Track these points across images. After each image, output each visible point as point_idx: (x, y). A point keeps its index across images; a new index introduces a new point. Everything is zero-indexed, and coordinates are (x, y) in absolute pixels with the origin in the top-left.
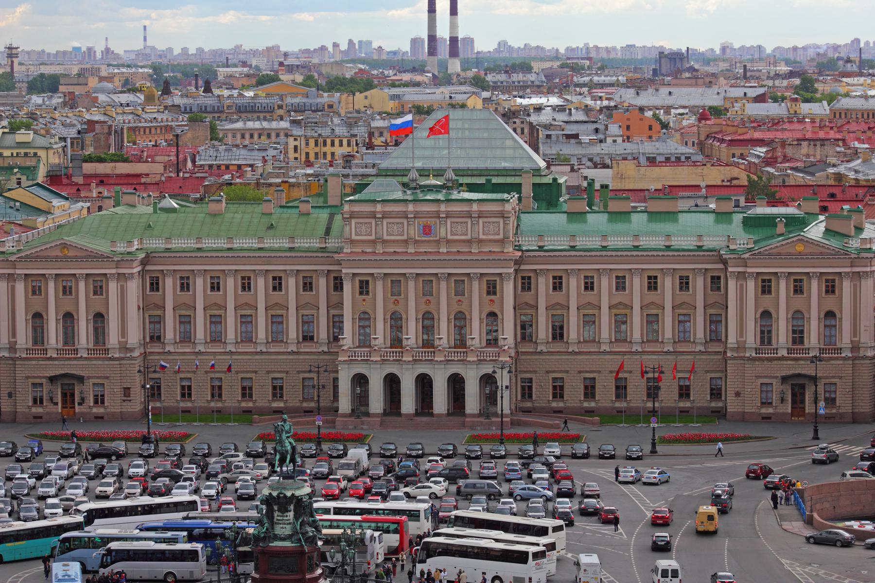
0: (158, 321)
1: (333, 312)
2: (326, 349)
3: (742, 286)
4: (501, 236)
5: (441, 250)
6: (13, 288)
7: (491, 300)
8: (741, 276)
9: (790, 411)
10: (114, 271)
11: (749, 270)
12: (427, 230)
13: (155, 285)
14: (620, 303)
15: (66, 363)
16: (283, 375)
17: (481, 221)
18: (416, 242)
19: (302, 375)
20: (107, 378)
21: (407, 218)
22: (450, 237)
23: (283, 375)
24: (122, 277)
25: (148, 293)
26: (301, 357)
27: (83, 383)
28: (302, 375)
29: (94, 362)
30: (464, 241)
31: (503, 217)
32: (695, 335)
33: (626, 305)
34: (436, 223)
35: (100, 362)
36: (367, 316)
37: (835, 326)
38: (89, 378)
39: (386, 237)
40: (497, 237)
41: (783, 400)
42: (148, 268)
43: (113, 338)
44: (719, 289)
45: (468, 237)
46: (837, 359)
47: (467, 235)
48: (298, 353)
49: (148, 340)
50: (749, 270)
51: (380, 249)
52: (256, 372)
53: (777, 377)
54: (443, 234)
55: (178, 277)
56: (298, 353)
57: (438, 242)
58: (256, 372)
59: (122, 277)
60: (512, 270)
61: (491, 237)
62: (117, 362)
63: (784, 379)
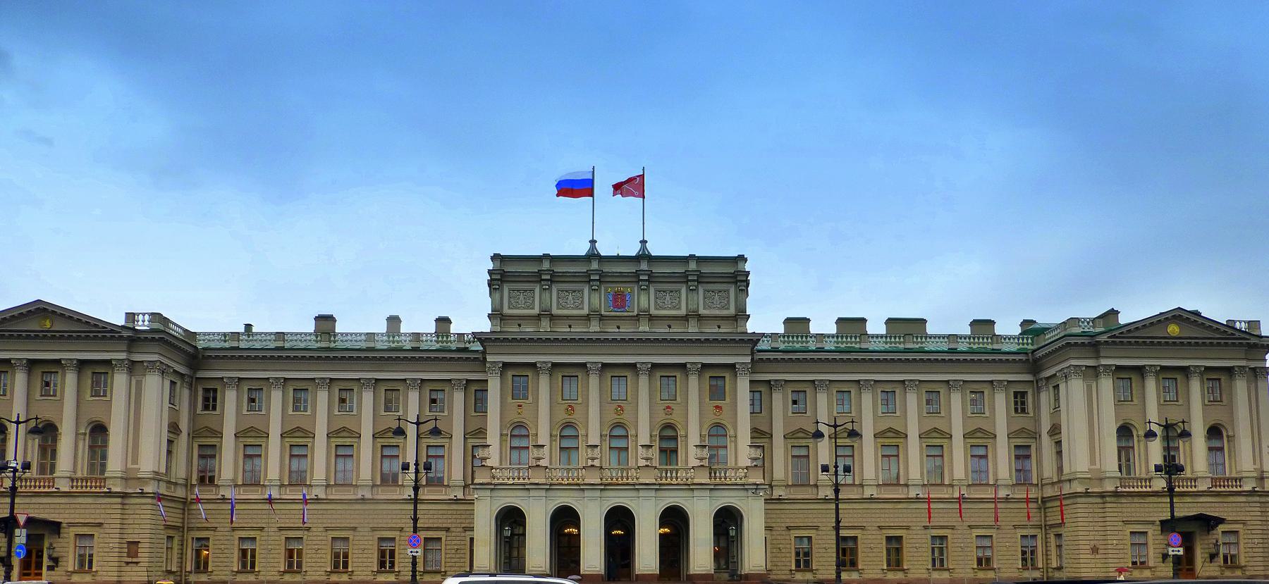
0: (209, 453)
1: (472, 442)
2: (460, 496)
4: (732, 311)
5: (641, 329)
7: (717, 407)
12: (619, 300)
13: (211, 400)
14: (890, 430)
15: (34, 500)
18: (602, 318)
20: (100, 525)
22: (653, 312)
25: (199, 411)
27: (59, 534)
29: (80, 500)
31: (736, 283)
32: (995, 474)
33: (897, 432)
34: (632, 291)
35: (90, 500)
36: (524, 432)
37: (1221, 449)
38: (71, 525)
39: (555, 311)
40: (725, 313)
42: (201, 374)
43: (114, 464)
44: (1023, 411)
45: (683, 312)
47: (679, 309)
51: (545, 325)
53: (1153, 523)
55: (246, 389)
57: (637, 318)
60: (748, 359)
61: (717, 312)
62: (119, 500)
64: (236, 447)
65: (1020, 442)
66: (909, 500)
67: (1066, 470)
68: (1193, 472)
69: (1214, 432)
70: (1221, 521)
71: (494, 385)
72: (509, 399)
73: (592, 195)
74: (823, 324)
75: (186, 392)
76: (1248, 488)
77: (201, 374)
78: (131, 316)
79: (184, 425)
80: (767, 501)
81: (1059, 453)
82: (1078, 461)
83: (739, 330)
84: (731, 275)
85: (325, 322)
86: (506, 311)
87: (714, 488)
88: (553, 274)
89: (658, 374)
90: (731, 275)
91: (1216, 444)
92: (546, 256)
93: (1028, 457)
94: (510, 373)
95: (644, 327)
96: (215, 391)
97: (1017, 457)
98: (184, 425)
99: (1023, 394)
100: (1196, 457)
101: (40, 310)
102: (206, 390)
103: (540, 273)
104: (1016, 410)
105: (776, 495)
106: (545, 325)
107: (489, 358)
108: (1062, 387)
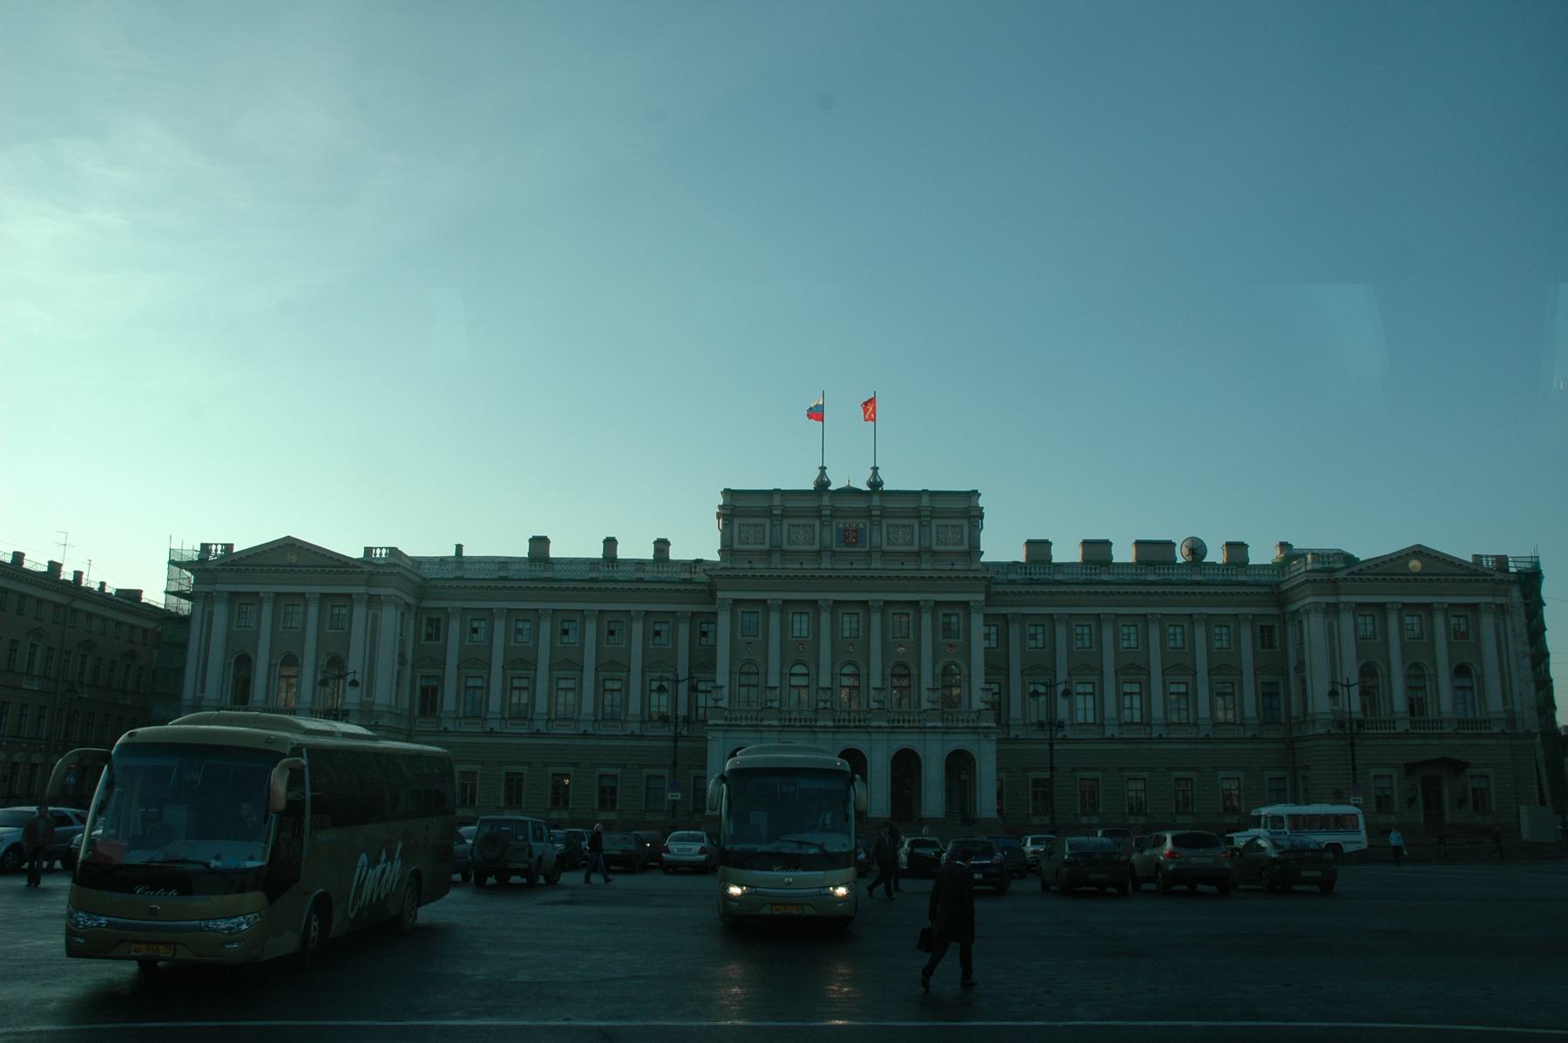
3: (1331, 625)
4: (965, 547)
5: (873, 565)
6: (211, 614)
8: (1333, 610)
9: (1421, 820)
10: (362, 590)
11: (1343, 599)
12: (850, 537)
13: (435, 629)
16: (617, 771)
17: (934, 523)
18: (834, 553)
19: (646, 772)
21: (820, 516)
22: (886, 547)
23: (617, 771)
24: (373, 601)
25: (423, 641)
26: (646, 743)
28: (646, 772)
30: (908, 553)
36: (753, 669)
37: (1471, 688)
39: (786, 547)
41: (1411, 802)
44: (1271, 646)
45: (915, 548)
46: (1481, 736)
48: (643, 737)
49: (416, 711)
50: (1343, 599)
51: (776, 561)
52: (575, 765)
54: (876, 541)
56: (643, 737)
58: (575, 765)
59: (373, 601)
60: (982, 597)
63: (1410, 768)
64: (458, 680)
65: (1266, 678)
66: (1151, 740)
67: (1310, 711)
68: (1439, 712)
69: (1461, 671)
70: (1466, 765)
71: (724, 620)
72: (739, 637)
73: (822, 419)
74: (1066, 552)
75: (412, 622)
76: (1496, 730)
77: (425, 604)
78: (368, 550)
79: (409, 656)
80: (999, 741)
81: (1304, 691)
82: (1321, 704)
83: (974, 567)
84: (963, 511)
85: (539, 544)
86: (736, 546)
87: (947, 730)
88: (784, 509)
89: (891, 611)
90: (963, 511)
91: (1466, 682)
92: (777, 491)
93: (1277, 694)
94: (740, 610)
95: (876, 564)
96: (439, 620)
97: (1264, 694)
98: (409, 656)
99: (1270, 629)
100: (1445, 697)
101: (289, 545)
102: (430, 621)
103: (770, 508)
104: (1263, 646)
105: (1013, 734)
106: (776, 561)
107: (720, 595)
108: (1305, 623)
